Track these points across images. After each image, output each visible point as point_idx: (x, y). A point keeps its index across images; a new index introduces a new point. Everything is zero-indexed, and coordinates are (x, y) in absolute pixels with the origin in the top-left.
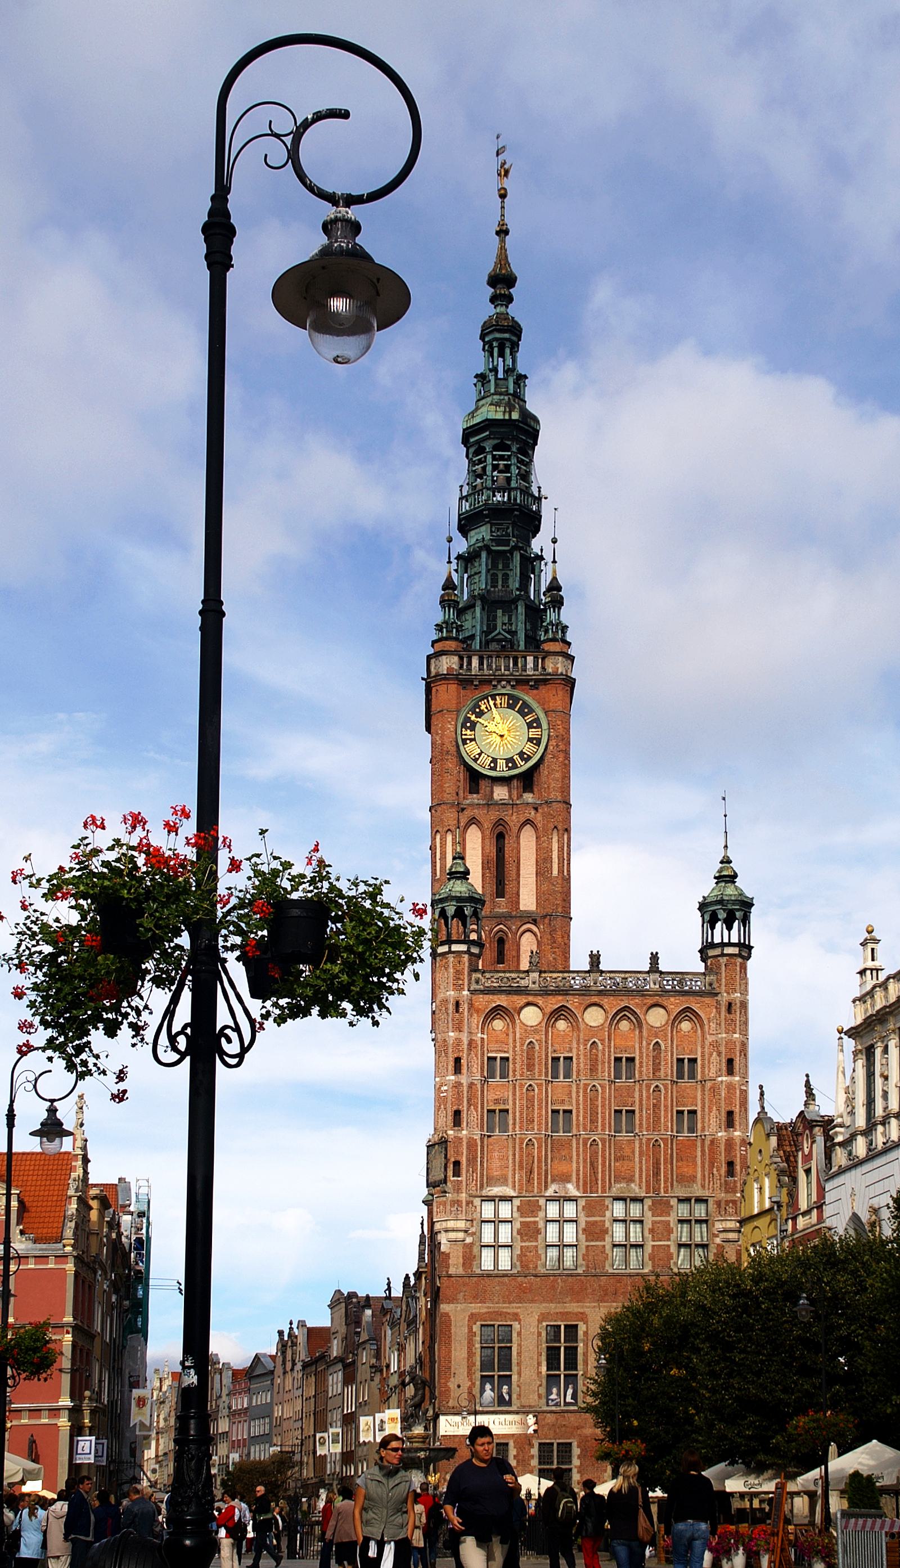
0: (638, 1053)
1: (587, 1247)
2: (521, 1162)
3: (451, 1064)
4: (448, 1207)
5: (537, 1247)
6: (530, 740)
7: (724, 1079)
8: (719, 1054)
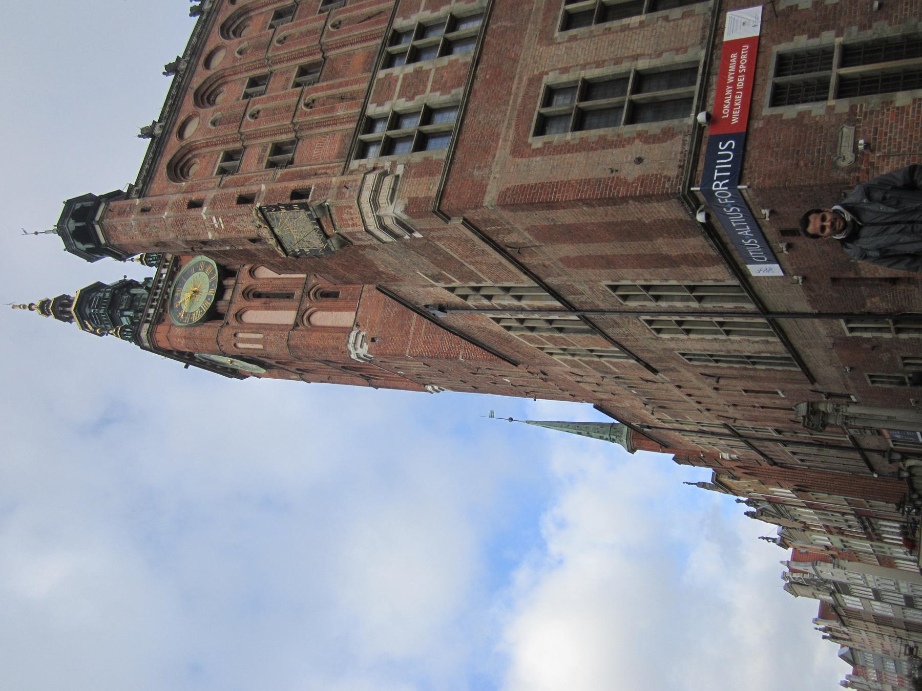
0: (270, 7)
3: (193, 212)
5: (437, 69)
6: (205, 268)
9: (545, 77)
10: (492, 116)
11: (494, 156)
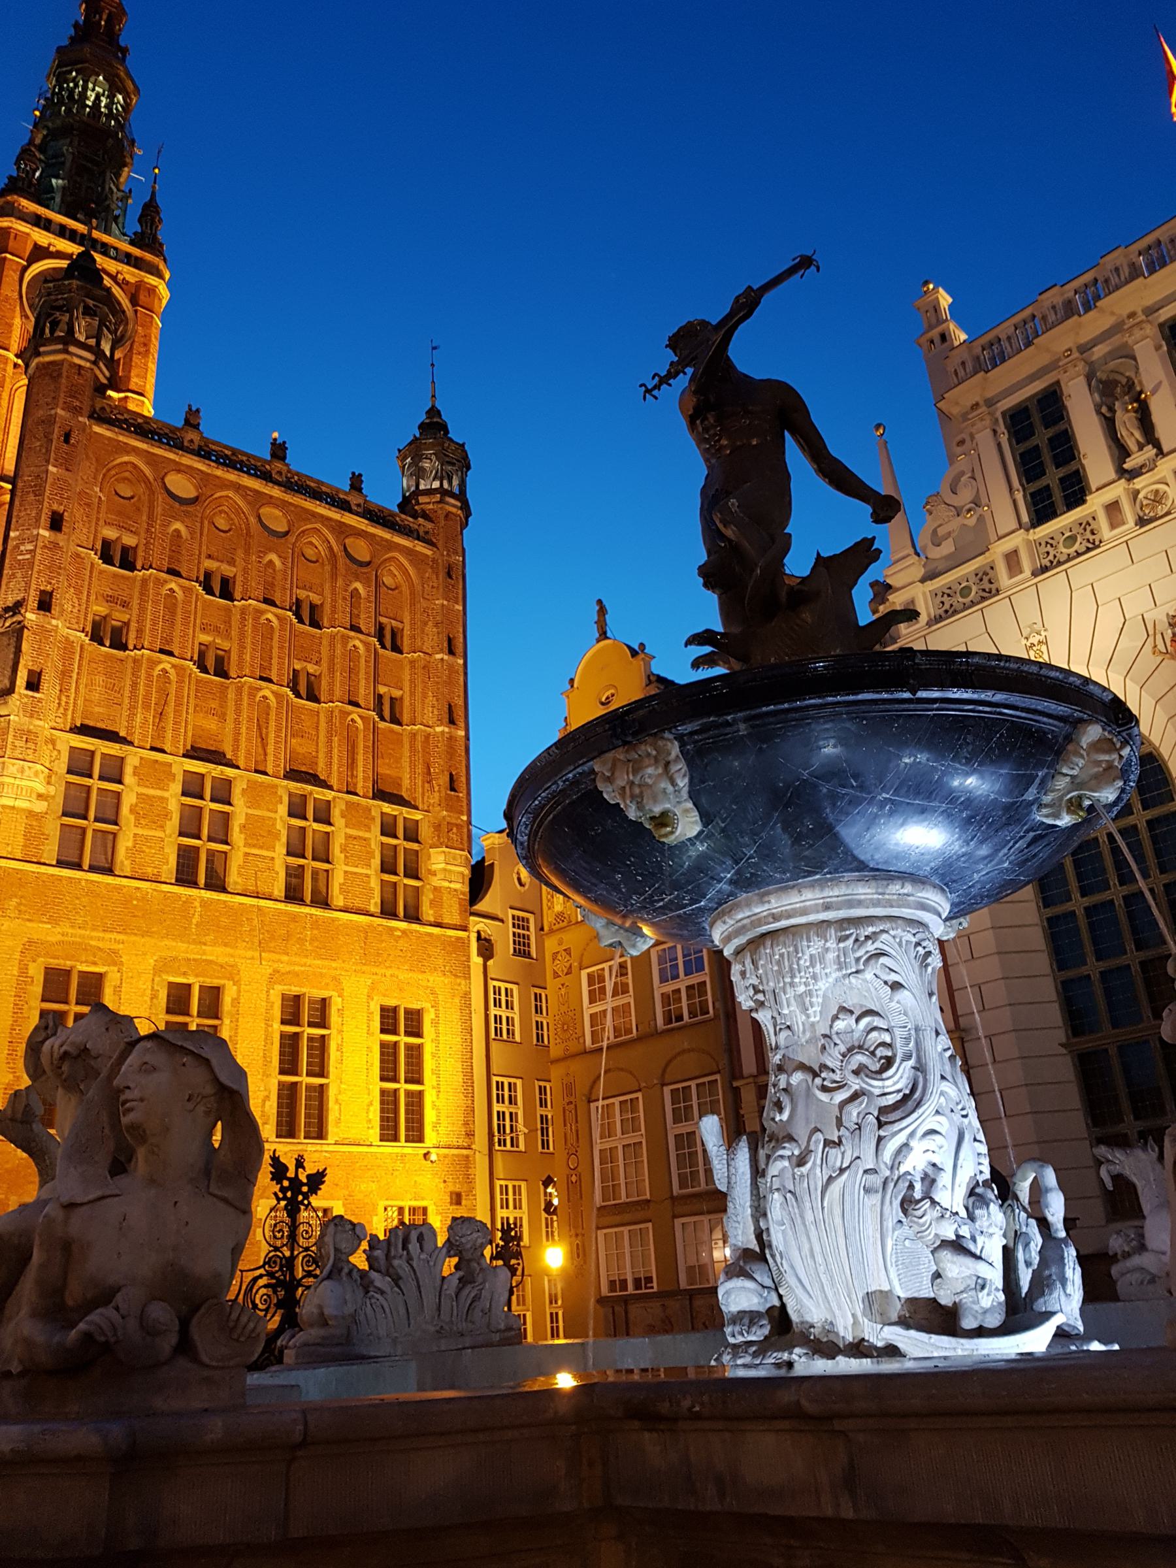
1: (247, 854)
2: (147, 696)
4: (10, 739)
7: (446, 657)
8: (436, 625)
9: (116, 969)
10: (82, 913)
11: (29, 920)
